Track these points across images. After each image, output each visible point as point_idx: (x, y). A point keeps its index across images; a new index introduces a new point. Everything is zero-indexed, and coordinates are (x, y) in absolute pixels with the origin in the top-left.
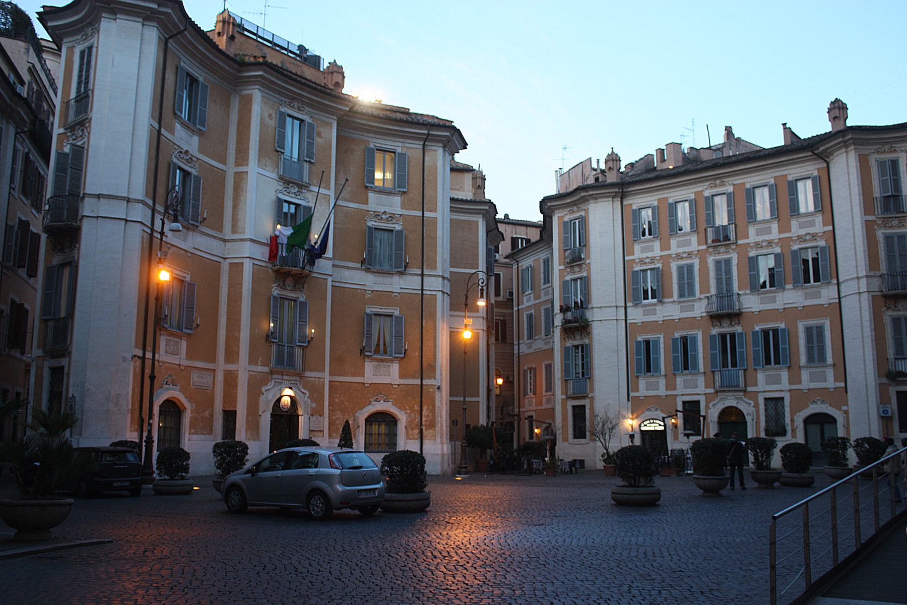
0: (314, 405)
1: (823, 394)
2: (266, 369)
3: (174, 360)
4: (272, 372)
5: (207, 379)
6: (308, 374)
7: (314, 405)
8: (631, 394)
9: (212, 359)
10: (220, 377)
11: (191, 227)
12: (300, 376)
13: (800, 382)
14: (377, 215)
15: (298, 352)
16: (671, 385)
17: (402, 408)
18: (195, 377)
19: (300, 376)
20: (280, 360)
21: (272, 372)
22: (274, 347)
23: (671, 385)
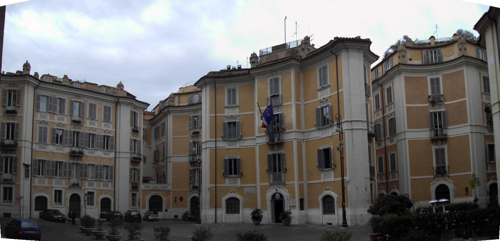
0: (291, 196)
2: (268, 184)
3: (235, 185)
4: (271, 184)
5: (254, 190)
6: (287, 183)
7: (291, 196)
9: (255, 182)
10: (259, 188)
11: (241, 139)
12: (284, 184)
14: (321, 102)
15: (283, 174)
17: (336, 193)
18: (246, 190)
19: (284, 184)
20: (275, 179)
21: (271, 184)
22: (272, 175)
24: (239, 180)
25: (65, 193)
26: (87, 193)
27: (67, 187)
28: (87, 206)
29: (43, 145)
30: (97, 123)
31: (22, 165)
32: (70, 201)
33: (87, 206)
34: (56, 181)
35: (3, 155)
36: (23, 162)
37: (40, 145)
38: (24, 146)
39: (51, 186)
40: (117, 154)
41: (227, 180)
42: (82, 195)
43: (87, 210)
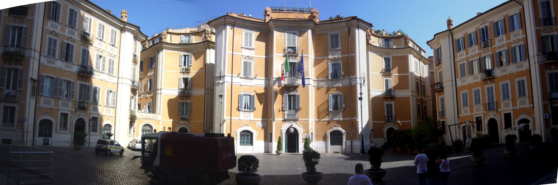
1: (525, 111)
8: (460, 115)
13: (516, 106)
16: (472, 111)
23: (472, 111)
24: (252, 114)
25: (71, 117)
26: (91, 117)
27: (74, 110)
28: (91, 133)
29: (52, 60)
30: (104, 44)
31: (30, 80)
32: (75, 126)
33: (91, 133)
34: (62, 103)
35: (6, 66)
36: (30, 76)
37: (49, 59)
38: (32, 56)
39: (57, 108)
40: (120, 79)
41: (241, 113)
42: (87, 120)
43: (91, 137)
